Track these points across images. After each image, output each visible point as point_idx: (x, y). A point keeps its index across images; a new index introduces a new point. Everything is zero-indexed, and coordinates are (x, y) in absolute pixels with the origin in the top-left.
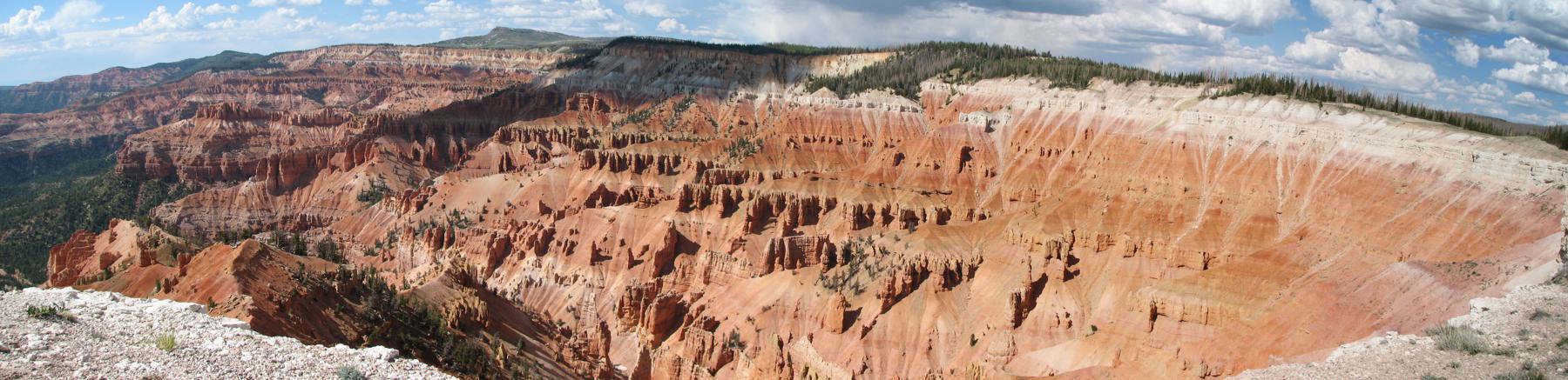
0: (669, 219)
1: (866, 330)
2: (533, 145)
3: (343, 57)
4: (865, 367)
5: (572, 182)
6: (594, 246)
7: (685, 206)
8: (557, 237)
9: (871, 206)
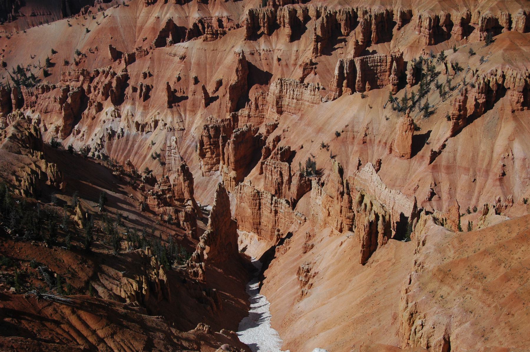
0: (238, 49)
1: (434, 155)
4: (433, 194)
5: (140, 21)
6: (169, 87)
7: (253, 35)
8: (131, 82)
9: (448, 16)
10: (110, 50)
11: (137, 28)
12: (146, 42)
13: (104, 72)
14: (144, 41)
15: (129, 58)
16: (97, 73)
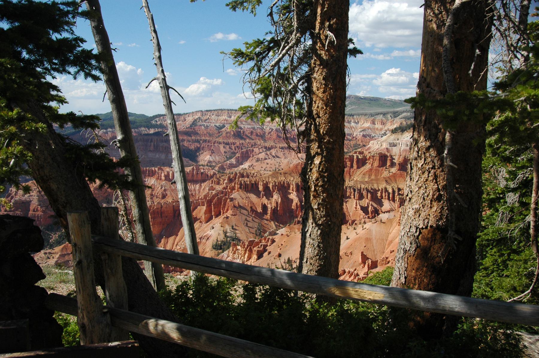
2: (365, 202)
3: (215, 121)
10: (362, 255)
11: (388, 241)
12: (393, 253)
13: (349, 272)
14: (391, 252)
15: (371, 265)
16: (344, 272)
